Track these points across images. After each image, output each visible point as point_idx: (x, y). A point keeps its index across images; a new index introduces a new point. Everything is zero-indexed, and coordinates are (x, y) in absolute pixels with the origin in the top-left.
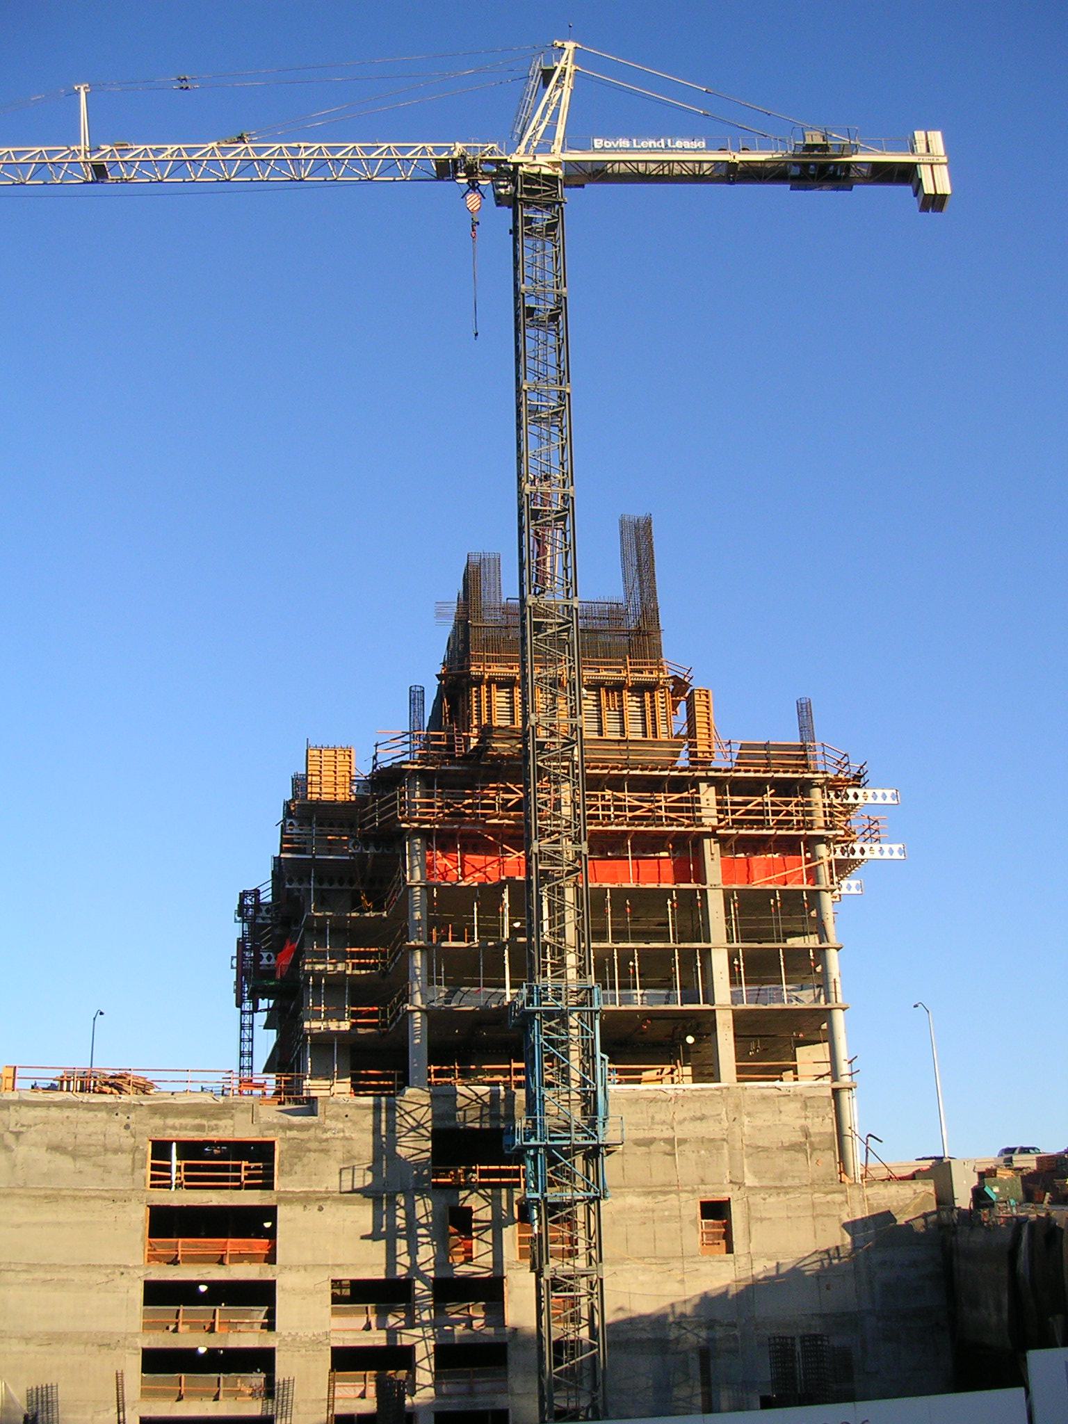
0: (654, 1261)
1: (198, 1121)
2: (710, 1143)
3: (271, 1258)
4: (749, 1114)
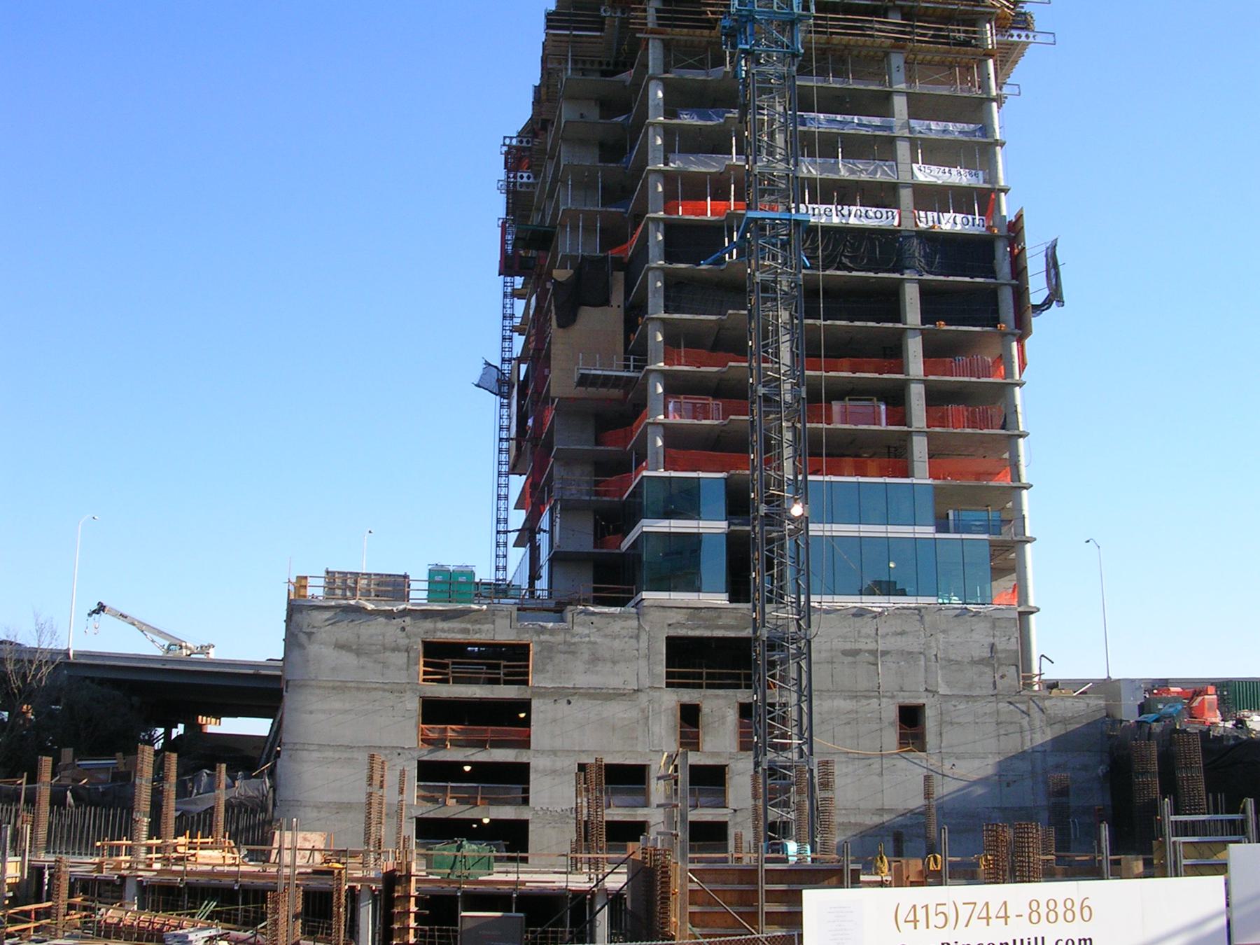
1: (463, 625)
2: (909, 655)
3: (525, 744)
4: (943, 632)
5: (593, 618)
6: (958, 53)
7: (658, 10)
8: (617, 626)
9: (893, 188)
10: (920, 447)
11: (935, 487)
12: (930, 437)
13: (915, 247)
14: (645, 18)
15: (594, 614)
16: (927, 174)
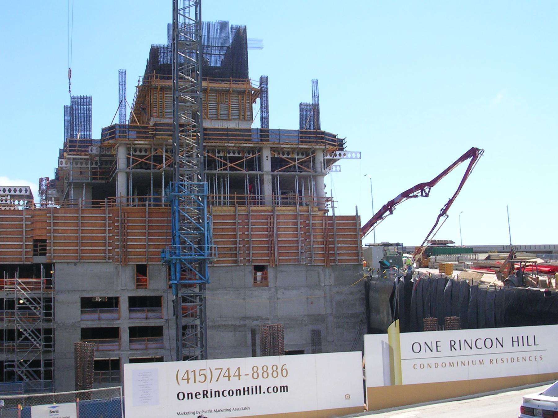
0: (231, 289)
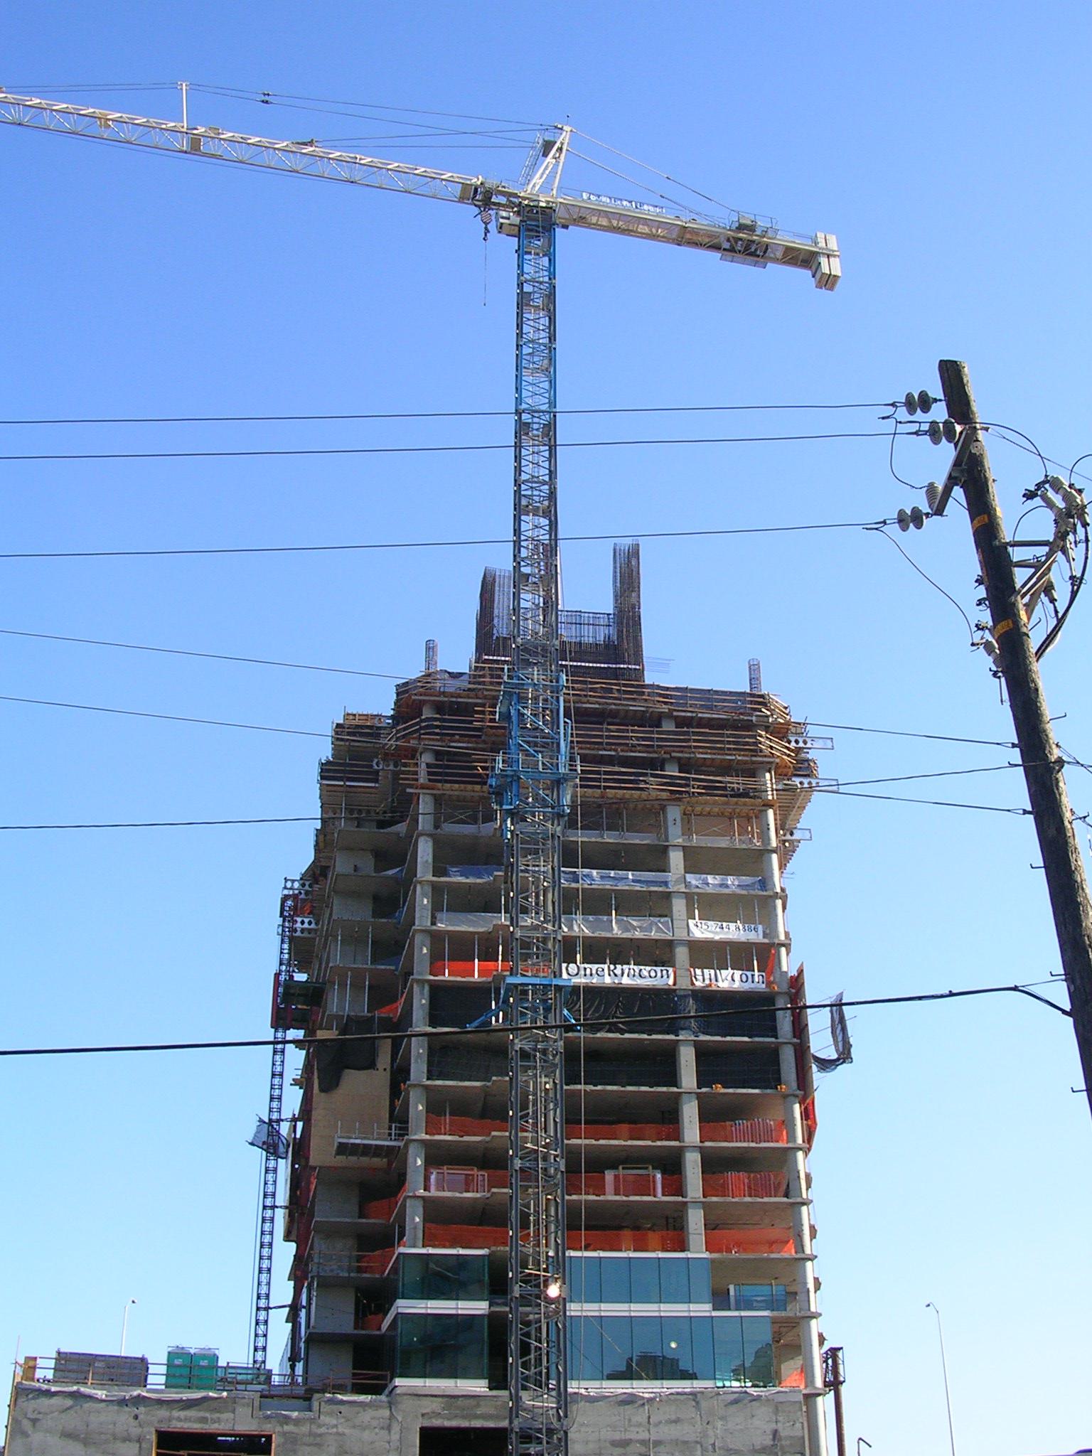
1: (202, 1414)
4: (723, 1418)
5: (342, 1408)
6: (736, 803)
7: (428, 765)
8: (366, 1416)
9: (670, 945)
10: (696, 1220)
11: (713, 1261)
12: (707, 1207)
13: (692, 1007)
14: (416, 773)
15: (342, 1402)
16: (704, 930)
